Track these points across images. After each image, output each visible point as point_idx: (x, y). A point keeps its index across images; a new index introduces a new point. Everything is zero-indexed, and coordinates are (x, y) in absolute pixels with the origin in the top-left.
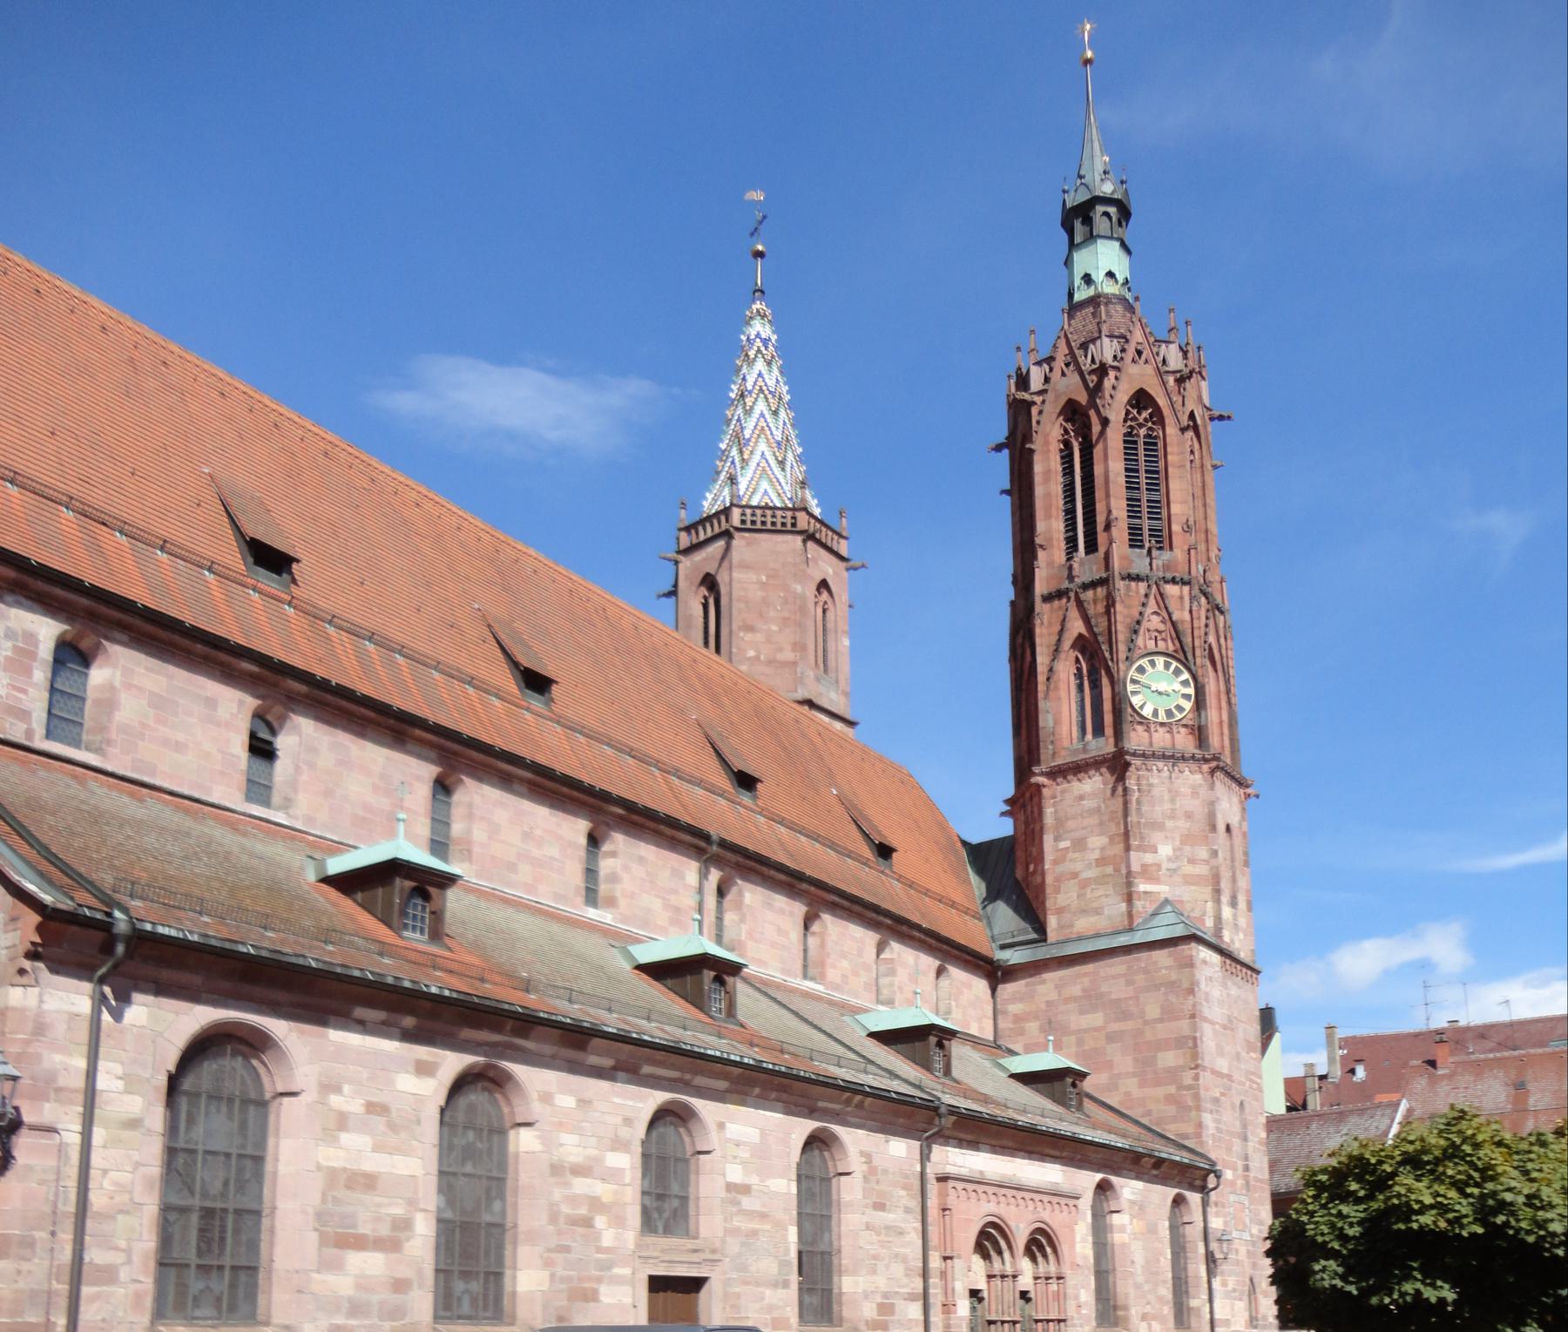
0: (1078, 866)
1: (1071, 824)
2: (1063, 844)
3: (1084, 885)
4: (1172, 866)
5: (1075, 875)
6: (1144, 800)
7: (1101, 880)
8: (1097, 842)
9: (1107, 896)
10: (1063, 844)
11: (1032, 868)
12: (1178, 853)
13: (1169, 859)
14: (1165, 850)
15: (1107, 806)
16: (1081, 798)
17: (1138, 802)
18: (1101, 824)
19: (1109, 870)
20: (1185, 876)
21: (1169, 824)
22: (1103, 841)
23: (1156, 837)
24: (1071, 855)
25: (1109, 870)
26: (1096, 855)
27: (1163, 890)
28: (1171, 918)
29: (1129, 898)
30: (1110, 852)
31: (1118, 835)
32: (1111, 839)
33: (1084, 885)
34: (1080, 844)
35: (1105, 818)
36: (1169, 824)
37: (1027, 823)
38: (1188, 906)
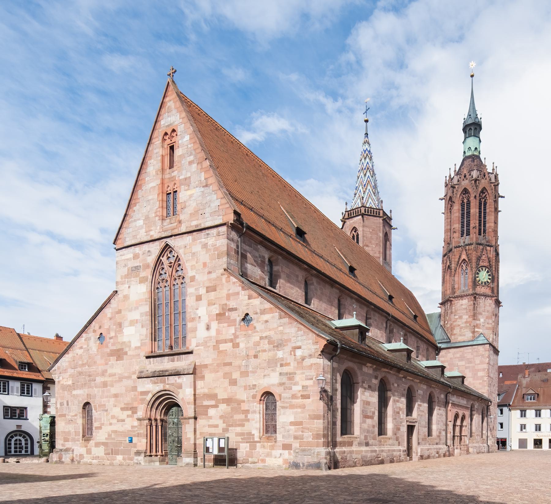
0: (460, 323)
1: (458, 312)
2: (456, 317)
3: (461, 328)
4: (483, 324)
5: (459, 325)
6: (478, 307)
7: (466, 327)
8: (465, 317)
9: (467, 331)
10: (456, 317)
11: (446, 322)
12: (485, 321)
13: (483, 323)
14: (482, 320)
15: (468, 308)
16: (462, 305)
17: (477, 307)
18: (467, 312)
19: (468, 325)
20: (486, 327)
21: (483, 313)
22: (467, 317)
23: (480, 317)
24: (458, 320)
25: (468, 325)
26: (465, 320)
27: (481, 331)
28: (484, 338)
29: (474, 332)
30: (469, 320)
31: (471, 315)
32: (469, 317)
33: (461, 328)
34: (461, 317)
35: (468, 311)
36: (483, 313)
37: (445, 310)
38: (486, 335)
